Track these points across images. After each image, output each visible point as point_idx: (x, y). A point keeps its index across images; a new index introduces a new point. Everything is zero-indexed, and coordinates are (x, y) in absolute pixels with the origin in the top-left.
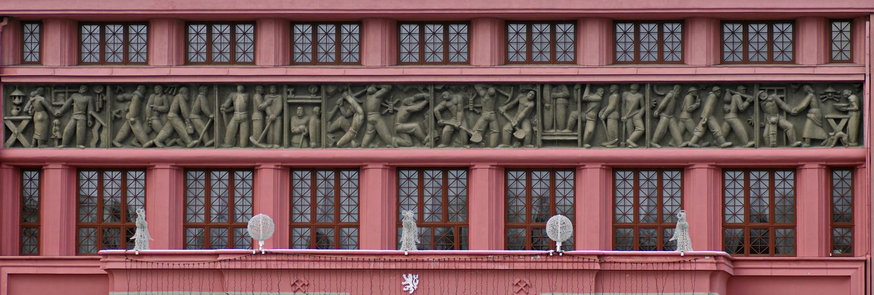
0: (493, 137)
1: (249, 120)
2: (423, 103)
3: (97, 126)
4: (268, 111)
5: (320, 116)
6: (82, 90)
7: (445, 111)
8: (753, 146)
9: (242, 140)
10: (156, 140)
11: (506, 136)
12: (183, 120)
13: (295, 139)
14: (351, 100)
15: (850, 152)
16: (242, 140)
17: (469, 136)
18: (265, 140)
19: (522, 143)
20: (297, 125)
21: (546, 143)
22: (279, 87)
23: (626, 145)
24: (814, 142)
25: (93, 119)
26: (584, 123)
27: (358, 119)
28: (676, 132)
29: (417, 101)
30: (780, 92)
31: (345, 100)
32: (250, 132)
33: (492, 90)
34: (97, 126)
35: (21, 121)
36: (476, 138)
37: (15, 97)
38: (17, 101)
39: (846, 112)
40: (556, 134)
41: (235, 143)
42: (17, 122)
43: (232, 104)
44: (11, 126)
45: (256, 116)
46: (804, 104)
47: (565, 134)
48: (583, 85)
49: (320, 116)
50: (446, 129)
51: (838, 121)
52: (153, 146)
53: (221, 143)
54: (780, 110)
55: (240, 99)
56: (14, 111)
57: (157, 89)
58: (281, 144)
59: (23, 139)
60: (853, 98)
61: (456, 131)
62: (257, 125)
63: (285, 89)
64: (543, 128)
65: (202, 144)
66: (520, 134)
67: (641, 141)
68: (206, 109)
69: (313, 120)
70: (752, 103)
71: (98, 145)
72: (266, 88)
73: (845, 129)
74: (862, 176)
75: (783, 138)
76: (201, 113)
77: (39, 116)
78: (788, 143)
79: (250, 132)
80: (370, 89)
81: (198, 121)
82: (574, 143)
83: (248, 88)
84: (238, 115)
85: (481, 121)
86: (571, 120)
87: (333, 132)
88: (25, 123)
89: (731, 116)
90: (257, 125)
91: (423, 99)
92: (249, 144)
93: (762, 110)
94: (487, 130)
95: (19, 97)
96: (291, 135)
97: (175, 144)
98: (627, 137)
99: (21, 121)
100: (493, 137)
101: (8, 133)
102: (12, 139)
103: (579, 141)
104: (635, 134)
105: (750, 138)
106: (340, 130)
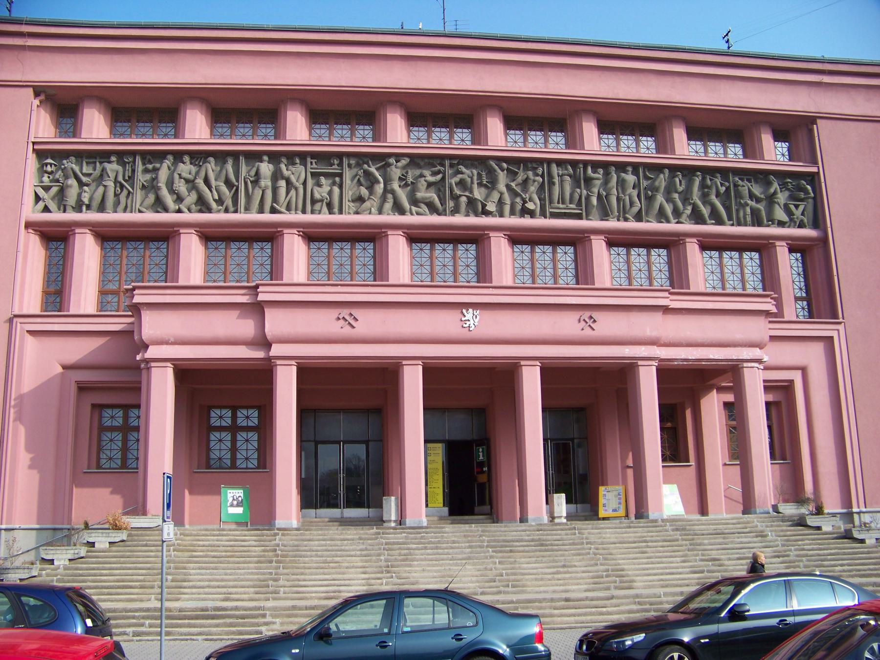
0: (507, 209)
1: (275, 190)
2: (440, 176)
3: (125, 192)
4: (293, 179)
5: (341, 187)
6: (113, 159)
7: (462, 184)
8: (732, 225)
9: (267, 207)
10: (182, 207)
11: (519, 207)
12: (209, 187)
13: (317, 206)
14: (373, 169)
15: (809, 232)
16: (267, 207)
17: (484, 206)
18: (288, 208)
19: (532, 214)
20: (321, 192)
21: (554, 215)
22: (303, 156)
23: (626, 220)
24: (781, 224)
25: (122, 187)
26: (588, 198)
27: (380, 188)
28: (669, 209)
29: (434, 174)
30: (749, 181)
31: (367, 174)
32: (275, 199)
33: (505, 165)
34: (125, 192)
35: (51, 187)
36: (491, 207)
37: (46, 165)
38: (49, 169)
39: (802, 200)
40: (561, 208)
41: (261, 211)
42: (47, 189)
43: (257, 174)
44: (41, 193)
45: (282, 183)
46: (772, 190)
47: (573, 208)
48: (586, 163)
49: (341, 187)
50: (464, 200)
51: (797, 207)
52: (179, 211)
53: (247, 209)
54: (752, 196)
55: (266, 168)
56: (46, 179)
57: (187, 159)
58: (304, 211)
59: (52, 206)
60: (809, 187)
61: (471, 202)
62: (283, 191)
63: (309, 160)
64: (551, 202)
65: (226, 211)
66: (530, 206)
67: (639, 217)
68: (232, 177)
69: (336, 190)
70: (728, 189)
71: (125, 210)
72: (291, 157)
73: (803, 214)
74: (817, 253)
75: (757, 221)
76: (228, 182)
77: (72, 182)
78: (760, 224)
79: (275, 199)
80: (392, 160)
81: (224, 189)
82: (579, 217)
83: (274, 157)
84: (266, 182)
85: (496, 196)
86: (577, 196)
87: (353, 201)
88: (54, 190)
89: (713, 197)
90: (283, 191)
91: (439, 172)
92: (273, 211)
93: (739, 195)
94: (500, 203)
95: (51, 165)
96: (314, 202)
97: (201, 211)
98: (625, 212)
99: (51, 187)
100: (507, 209)
101: (38, 198)
102: (41, 205)
103: (584, 214)
104: (635, 209)
105: (730, 218)
106: (360, 200)
